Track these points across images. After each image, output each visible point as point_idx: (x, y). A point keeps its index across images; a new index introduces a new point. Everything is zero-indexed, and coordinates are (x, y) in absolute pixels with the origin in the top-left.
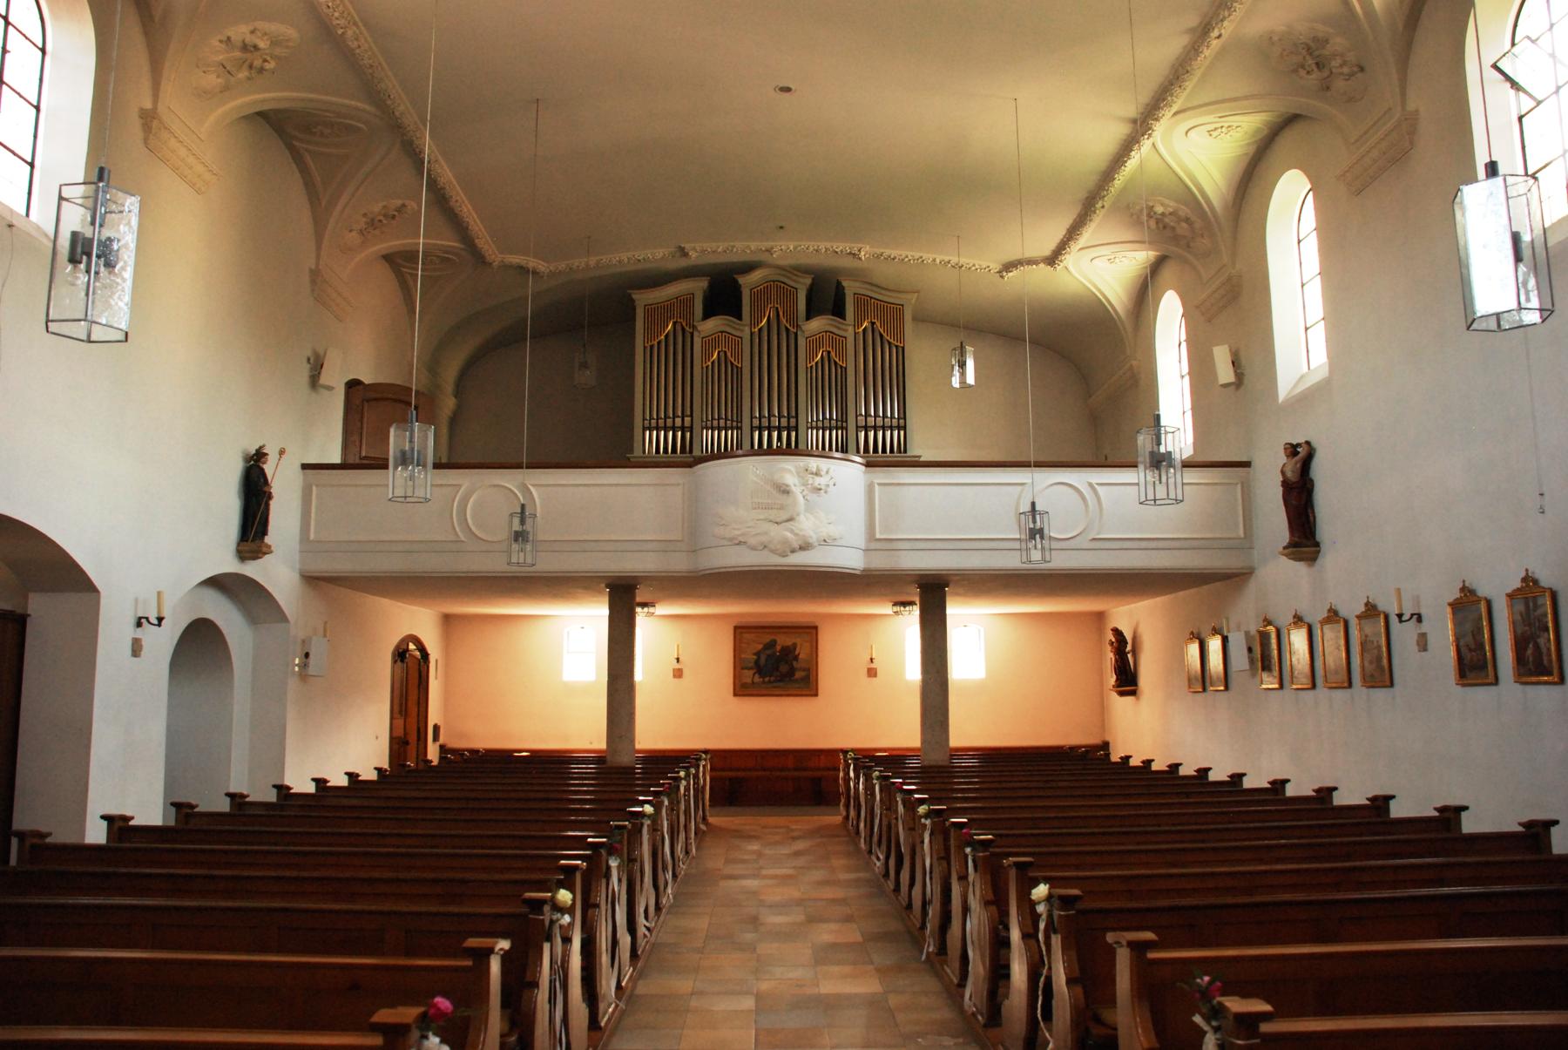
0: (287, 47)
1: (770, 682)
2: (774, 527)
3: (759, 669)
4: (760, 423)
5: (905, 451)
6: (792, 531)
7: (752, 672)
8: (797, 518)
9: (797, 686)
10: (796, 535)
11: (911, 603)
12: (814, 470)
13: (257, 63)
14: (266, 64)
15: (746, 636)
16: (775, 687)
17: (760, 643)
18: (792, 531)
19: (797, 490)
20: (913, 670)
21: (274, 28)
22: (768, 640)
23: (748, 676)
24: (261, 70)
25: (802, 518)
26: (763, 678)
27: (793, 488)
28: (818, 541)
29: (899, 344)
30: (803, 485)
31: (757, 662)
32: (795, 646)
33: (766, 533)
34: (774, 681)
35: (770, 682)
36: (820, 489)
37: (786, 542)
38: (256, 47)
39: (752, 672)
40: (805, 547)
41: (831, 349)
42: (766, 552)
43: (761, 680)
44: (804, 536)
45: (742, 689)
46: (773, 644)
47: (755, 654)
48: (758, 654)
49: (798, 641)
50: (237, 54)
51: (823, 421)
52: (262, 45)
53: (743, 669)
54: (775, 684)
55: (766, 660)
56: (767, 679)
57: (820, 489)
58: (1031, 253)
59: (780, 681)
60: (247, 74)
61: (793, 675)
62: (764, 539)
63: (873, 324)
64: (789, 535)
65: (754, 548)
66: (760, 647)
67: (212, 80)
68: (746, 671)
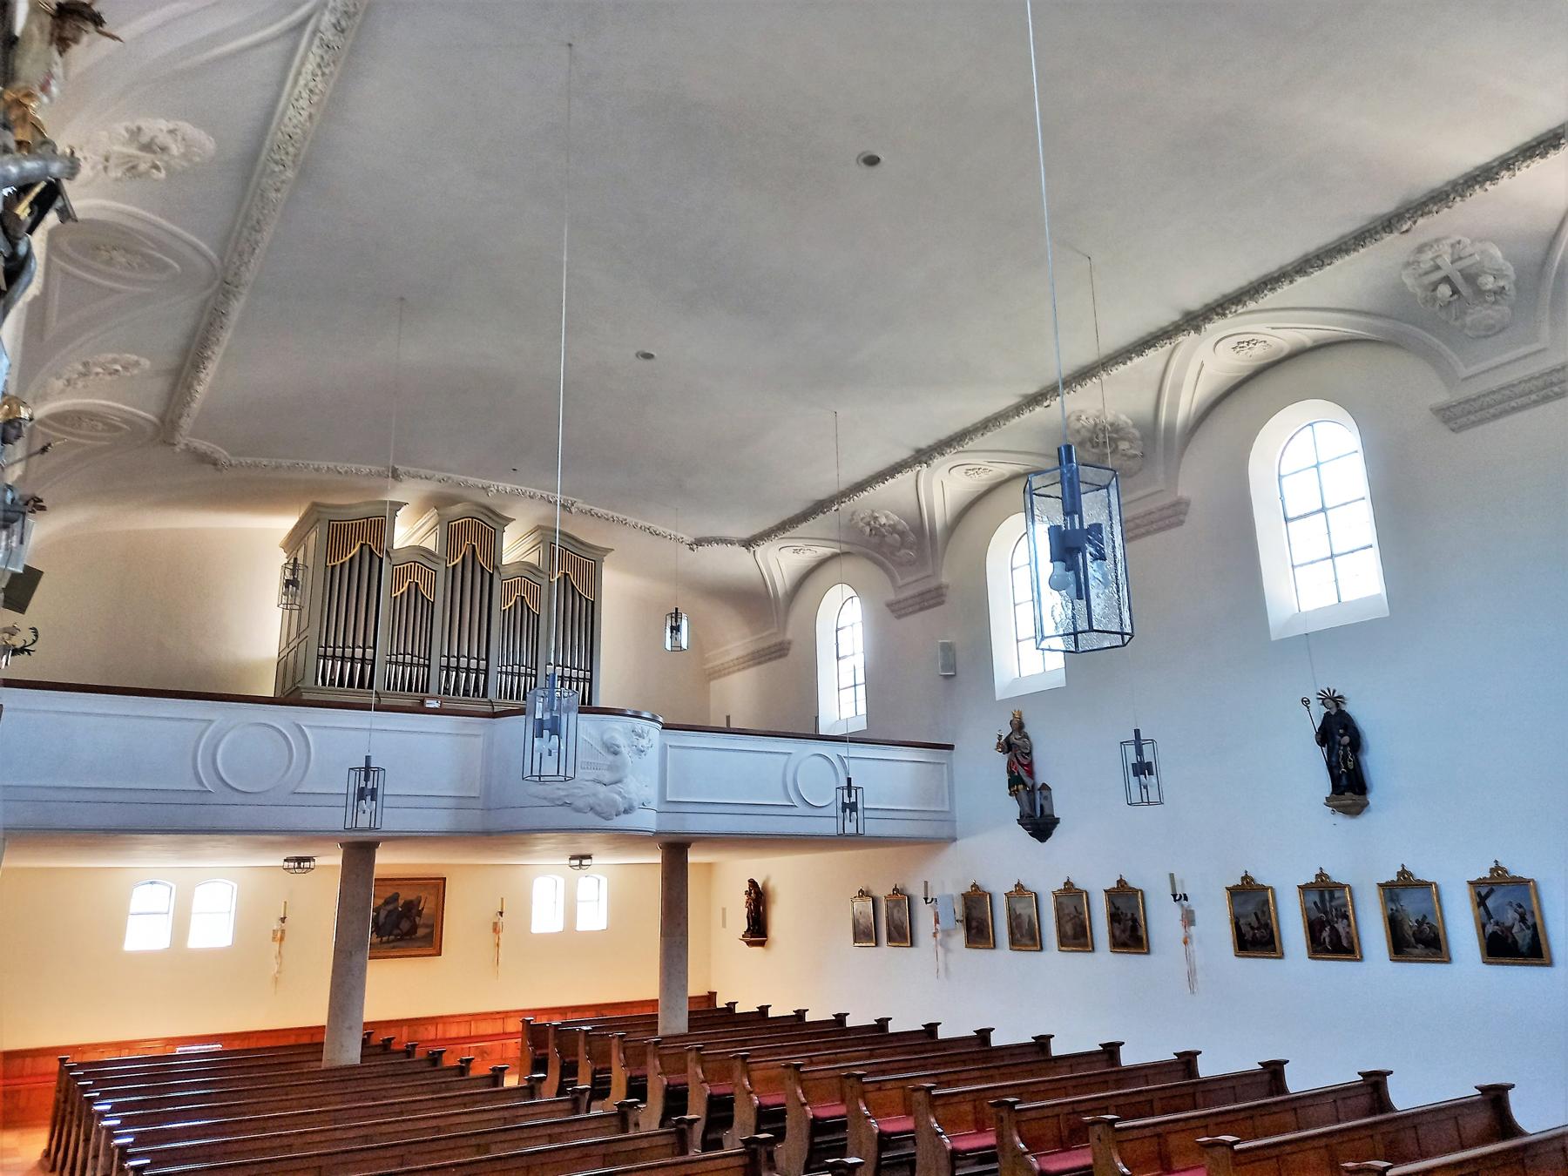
4: (468, 664)
10: (624, 798)
16: (394, 948)
19: (625, 750)
22: (388, 895)
26: (381, 937)
27: (623, 749)
28: (639, 804)
33: (594, 795)
34: (393, 941)
35: (388, 942)
37: (613, 803)
42: (590, 814)
43: (379, 939)
44: (630, 799)
54: (392, 945)
55: (387, 917)
56: (385, 939)
59: (399, 940)
62: (591, 800)
63: (566, 574)
65: (578, 810)
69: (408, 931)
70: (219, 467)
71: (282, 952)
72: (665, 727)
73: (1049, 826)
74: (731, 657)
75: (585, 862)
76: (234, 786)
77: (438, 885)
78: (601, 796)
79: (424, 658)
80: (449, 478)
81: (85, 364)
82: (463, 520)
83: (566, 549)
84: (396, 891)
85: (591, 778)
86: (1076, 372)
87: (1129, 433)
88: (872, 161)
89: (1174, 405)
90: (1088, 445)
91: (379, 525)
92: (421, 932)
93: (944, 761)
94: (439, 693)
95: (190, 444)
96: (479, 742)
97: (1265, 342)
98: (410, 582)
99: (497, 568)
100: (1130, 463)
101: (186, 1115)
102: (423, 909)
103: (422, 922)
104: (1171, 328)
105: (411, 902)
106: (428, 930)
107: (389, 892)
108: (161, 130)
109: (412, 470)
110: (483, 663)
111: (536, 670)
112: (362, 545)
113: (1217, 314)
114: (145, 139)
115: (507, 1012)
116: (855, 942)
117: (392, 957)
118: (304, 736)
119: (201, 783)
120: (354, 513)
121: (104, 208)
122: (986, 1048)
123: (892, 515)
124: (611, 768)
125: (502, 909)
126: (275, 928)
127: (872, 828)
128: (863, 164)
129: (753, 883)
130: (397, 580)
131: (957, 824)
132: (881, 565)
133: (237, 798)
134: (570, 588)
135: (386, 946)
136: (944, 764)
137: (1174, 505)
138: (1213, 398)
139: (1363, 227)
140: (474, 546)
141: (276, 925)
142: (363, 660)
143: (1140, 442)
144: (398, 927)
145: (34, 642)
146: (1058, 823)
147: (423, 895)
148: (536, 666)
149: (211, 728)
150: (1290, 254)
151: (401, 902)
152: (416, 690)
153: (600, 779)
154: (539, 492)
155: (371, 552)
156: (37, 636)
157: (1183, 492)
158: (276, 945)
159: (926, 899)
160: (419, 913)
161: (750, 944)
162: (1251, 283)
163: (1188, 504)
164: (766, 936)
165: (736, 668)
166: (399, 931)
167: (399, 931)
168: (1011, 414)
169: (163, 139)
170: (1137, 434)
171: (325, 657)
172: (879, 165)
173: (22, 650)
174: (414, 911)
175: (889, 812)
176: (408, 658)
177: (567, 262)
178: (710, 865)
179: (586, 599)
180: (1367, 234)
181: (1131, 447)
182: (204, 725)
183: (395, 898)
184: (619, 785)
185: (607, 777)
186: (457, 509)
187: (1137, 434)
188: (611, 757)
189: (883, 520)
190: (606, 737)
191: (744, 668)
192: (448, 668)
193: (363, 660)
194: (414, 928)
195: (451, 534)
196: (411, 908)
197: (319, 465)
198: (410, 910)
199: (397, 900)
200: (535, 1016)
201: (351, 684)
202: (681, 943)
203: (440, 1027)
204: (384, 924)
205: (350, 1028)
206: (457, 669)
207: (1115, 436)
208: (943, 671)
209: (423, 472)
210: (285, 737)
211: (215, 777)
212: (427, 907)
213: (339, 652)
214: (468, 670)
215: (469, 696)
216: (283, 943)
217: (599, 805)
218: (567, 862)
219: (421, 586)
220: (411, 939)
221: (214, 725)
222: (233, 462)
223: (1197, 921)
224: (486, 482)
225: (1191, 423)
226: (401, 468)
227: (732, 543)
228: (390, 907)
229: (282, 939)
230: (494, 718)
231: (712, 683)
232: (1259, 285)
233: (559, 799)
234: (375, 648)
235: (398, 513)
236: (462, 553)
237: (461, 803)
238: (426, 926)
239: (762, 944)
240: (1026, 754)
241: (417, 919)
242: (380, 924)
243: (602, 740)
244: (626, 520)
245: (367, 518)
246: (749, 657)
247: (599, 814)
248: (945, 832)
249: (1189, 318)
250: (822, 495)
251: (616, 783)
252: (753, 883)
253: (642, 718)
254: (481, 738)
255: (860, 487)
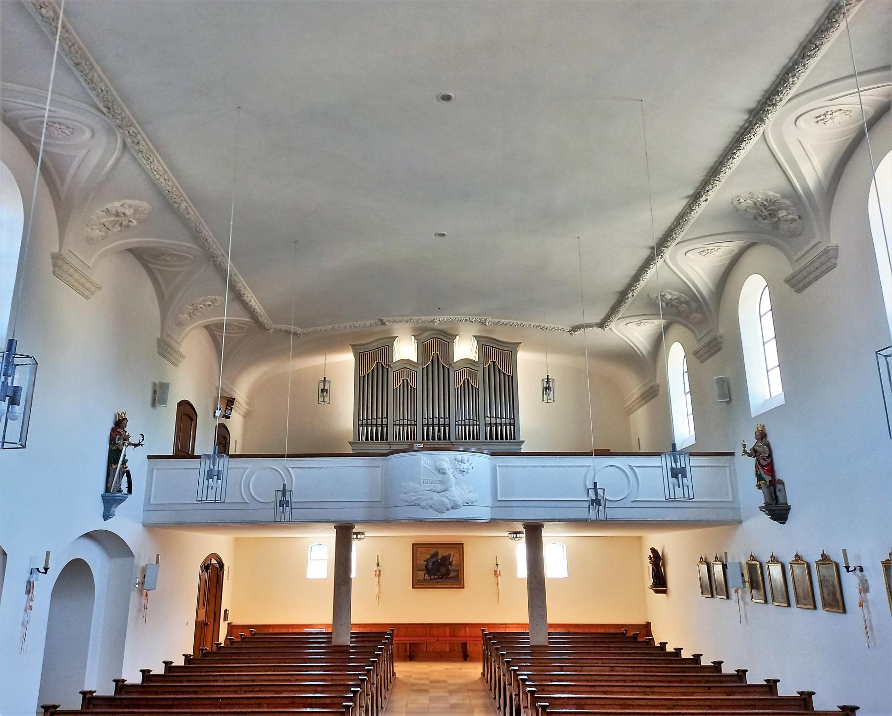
0: (144, 214)
1: (434, 579)
2: (435, 495)
3: (428, 571)
5: (514, 439)
6: (447, 497)
7: (423, 573)
8: (450, 489)
9: (452, 581)
10: (450, 500)
11: (521, 533)
12: (460, 459)
13: (124, 223)
14: (130, 223)
15: (419, 549)
16: (437, 582)
17: (428, 554)
18: (447, 497)
19: (450, 472)
20: (522, 571)
21: (136, 202)
23: (421, 575)
24: (128, 226)
25: (453, 488)
27: (448, 471)
28: (463, 503)
29: (509, 374)
30: (454, 469)
31: (427, 566)
32: (450, 555)
34: (438, 578)
35: (434, 579)
36: (464, 471)
37: (443, 504)
38: (124, 214)
39: (423, 573)
40: (455, 507)
41: (469, 378)
42: (431, 510)
43: (430, 577)
44: (454, 500)
45: (417, 584)
46: (436, 554)
47: (425, 561)
48: (427, 561)
49: (452, 553)
50: (113, 218)
51: (465, 420)
52: (128, 213)
53: (418, 570)
54: (437, 581)
56: (433, 577)
57: (464, 471)
58: (588, 320)
59: (440, 578)
60: (119, 229)
61: (449, 574)
62: (430, 502)
63: (494, 362)
64: (445, 499)
65: (423, 508)
66: (429, 556)
67: (97, 233)
68: (420, 572)
69: (445, 573)
70: (299, 335)
71: (380, 581)
72: (493, 454)
73: (783, 512)
74: (634, 398)
75: (518, 535)
76: (258, 500)
77: (459, 547)
78: (435, 499)
79: (411, 420)
80: (411, 319)
81: (192, 305)
82: (430, 340)
83: (493, 347)
84: (437, 550)
85: (429, 489)
86: (709, 172)
87: (782, 203)
88: (447, 98)
89: (800, 176)
90: (760, 219)
91: (387, 349)
92: (452, 574)
93: (726, 465)
94: (423, 439)
95: (277, 328)
96: (379, 471)
97: (840, 110)
98: (403, 380)
99: (451, 365)
100: (793, 225)
101: (316, 661)
102: (452, 561)
103: (452, 569)
104: (747, 125)
105: (445, 556)
106: (456, 573)
107: (433, 551)
108: (118, 207)
109: (390, 319)
110: (447, 422)
111: (479, 421)
112: (377, 363)
113: (770, 106)
114: (113, 212)
115: (507, 624)
116: (702, 594)
117: (437, 588)
118: (288, 469)
119: (243, 499)
120: (371, 347)
121: (139, 242)
122: (719, 674)
123: (673, 292)
124: (441, 482)
125: (497, 563)
126: (375, 569)
127: (612, 514)
128: (440, 100)
129: (653, 550)
130: (396, 380)
131: (742, 510)
132: (686, 326)
133: (261, 506)
134: (497, 370)
135: (434, 581)
136: (726, 467)
137: (826, 251)
138: (836, 162)
139: (827, 9)
140: (437, 354)
141: (375, 568)
142: (382, 425)
143: (794, 208)
144: (439, 571)
145: (143, 440)
146: (790, 509)
147: (452, 553)
148: (393, 427)
149: (247, 472)
150: (789, 47)
151: (440, 557)
152: (411, 439)
153: (434, 489)
154: (463, 318)
155: (382, 366)
156: (143, 438)
157: (834, 241)
158: (377, 578)
159: (847, 568)
160: (450, 563)
161: (657, 592)
162: (778, 76)
163: (836, 249)
164: (666, 587)
165: (637, 406)
166: (440, 574)
167: (440, 574)
168: (688, 211)
169: (120, 210)
170: (788, 202)
171: (362, 425)
172: (450, 101)
173: (139, 444)
174: (447, 562)
175: (648, 503)
176: (413, 422)
177: (233, 225)
178: (640, 537)
179: (508, 376)
180: (834, 12)
181: (789, 214)
182: (244, 470)
183: (436, 554)
184: (447, 492)
185: (439, 487)
186: (426, 334)
187: (788, 202)
188: (441, 476)
189: (669, 297)
190: (437, 464)
191: (643, 404)
192: (427, 425)
193: (382, 425)
194: (448, 572)
195: (423, 350)
196: (446, 560)
197: (345, 325)
198: (445, 562)
199: (437, 555)
200: (489, 628)
201: (372, 439)
202: (538, 588)
203: (467, 629)
204: (432, 569)
205: (341, 625)
206: (433, 425)
207: (773, 207)
208: (719, 398)
209: (396, 318)
210: (281, 474)
211: (251, 498)
212: (454, 560)
213: (369, 422)
214: (439, 425)
215: (435, 440)
216: (381, 577)
217: (434, 504)
218: (508, 535)
219: (409, 381)
220: (447, 578)
221: (248, 470)
222: (305, 332)
223: (871, 589)
224: (432, 318)
225: (825, 184)
226: (385, 319)
227: (592, 326)
228: (434, 560)
229: (379, 575)
230: (386, 456)
231: (631, 417)
232: (784, 76)
233: (413, 502)
234: (387, 417)
235: (394, 342)
236: (431, 359)
237: (371, 505)
238: (455, 571)
239: (665, 592)
240: (767, 457)
241: (450, 567)
242: (429, 569)
243: (435, 466)
244: (522, 324)
245: (379, 348)
246: (642, 397)
247: (436, 510)
248: (730, 516)
249: (753, 113)
250: (620, 287)
251: (444, 491)
252: (653, 550)
253: (472, 452)
254: (381, 468)
255: (636, 278)
